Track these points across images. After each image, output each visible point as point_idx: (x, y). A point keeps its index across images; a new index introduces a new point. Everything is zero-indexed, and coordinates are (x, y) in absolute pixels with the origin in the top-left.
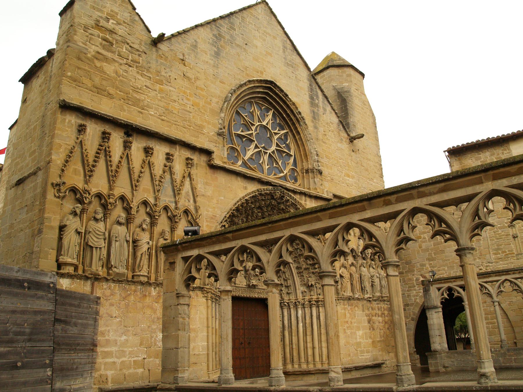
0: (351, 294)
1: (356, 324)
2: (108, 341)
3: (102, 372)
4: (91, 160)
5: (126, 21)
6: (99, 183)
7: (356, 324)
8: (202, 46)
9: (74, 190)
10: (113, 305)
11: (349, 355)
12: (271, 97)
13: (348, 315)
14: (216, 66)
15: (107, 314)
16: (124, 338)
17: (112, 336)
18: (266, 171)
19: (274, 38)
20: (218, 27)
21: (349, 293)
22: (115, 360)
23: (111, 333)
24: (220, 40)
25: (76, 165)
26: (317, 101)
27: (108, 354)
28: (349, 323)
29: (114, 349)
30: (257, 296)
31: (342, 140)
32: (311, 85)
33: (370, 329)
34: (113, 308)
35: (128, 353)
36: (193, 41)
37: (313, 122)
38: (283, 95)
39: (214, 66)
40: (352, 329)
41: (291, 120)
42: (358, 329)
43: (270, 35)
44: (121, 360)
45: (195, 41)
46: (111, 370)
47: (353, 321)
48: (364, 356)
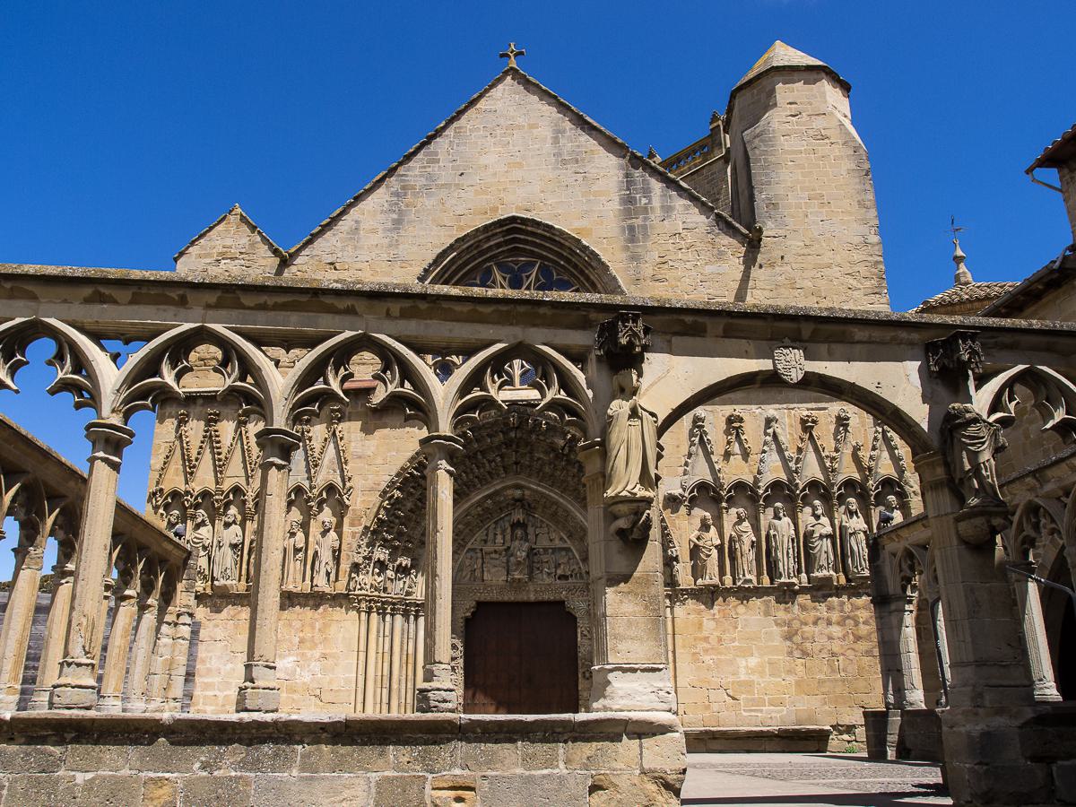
0: (716, 580)
1: (736, 644)
2: (209, 670)
3: (200, 707)
4: (194, 455)
5: (243, 250)
6: (204, 479)
7: (736, 644)
8: (367, 224)
9: (175, 494)
10: (218, 626)
11: (707, 708)
12: (526, 242)
13: (709, 625)
14: (394, 244)
15: (210, 636)
16: (229, 666)
17: (214, 664)
18: (517, 380)
19: (533, 126)
20: (402, 175)
21: (711, 577)
22: (217, 693)
23: (213, 661)
24: (405, 194)
25: (176, 464)
26: (644, 201)
27: (207, 686)
28: (713, 640)
29: (216, 680)
30: (532, 597)
31: (721, 253)
32: (627, 176)
33: (790, 653)
34: (217, 630)
35: (234, 684)
36: (353, 223)
37: (627, 249)
38: (544, 230)
39: (390, 246)
40: (720, 654)
41: (575, 266)
42: (746, 653)
43: (520, 127)
44: (225, 693)
45: (357, 222)
46: (211, 705)
47: (726, 636)
48: (761, 711)
